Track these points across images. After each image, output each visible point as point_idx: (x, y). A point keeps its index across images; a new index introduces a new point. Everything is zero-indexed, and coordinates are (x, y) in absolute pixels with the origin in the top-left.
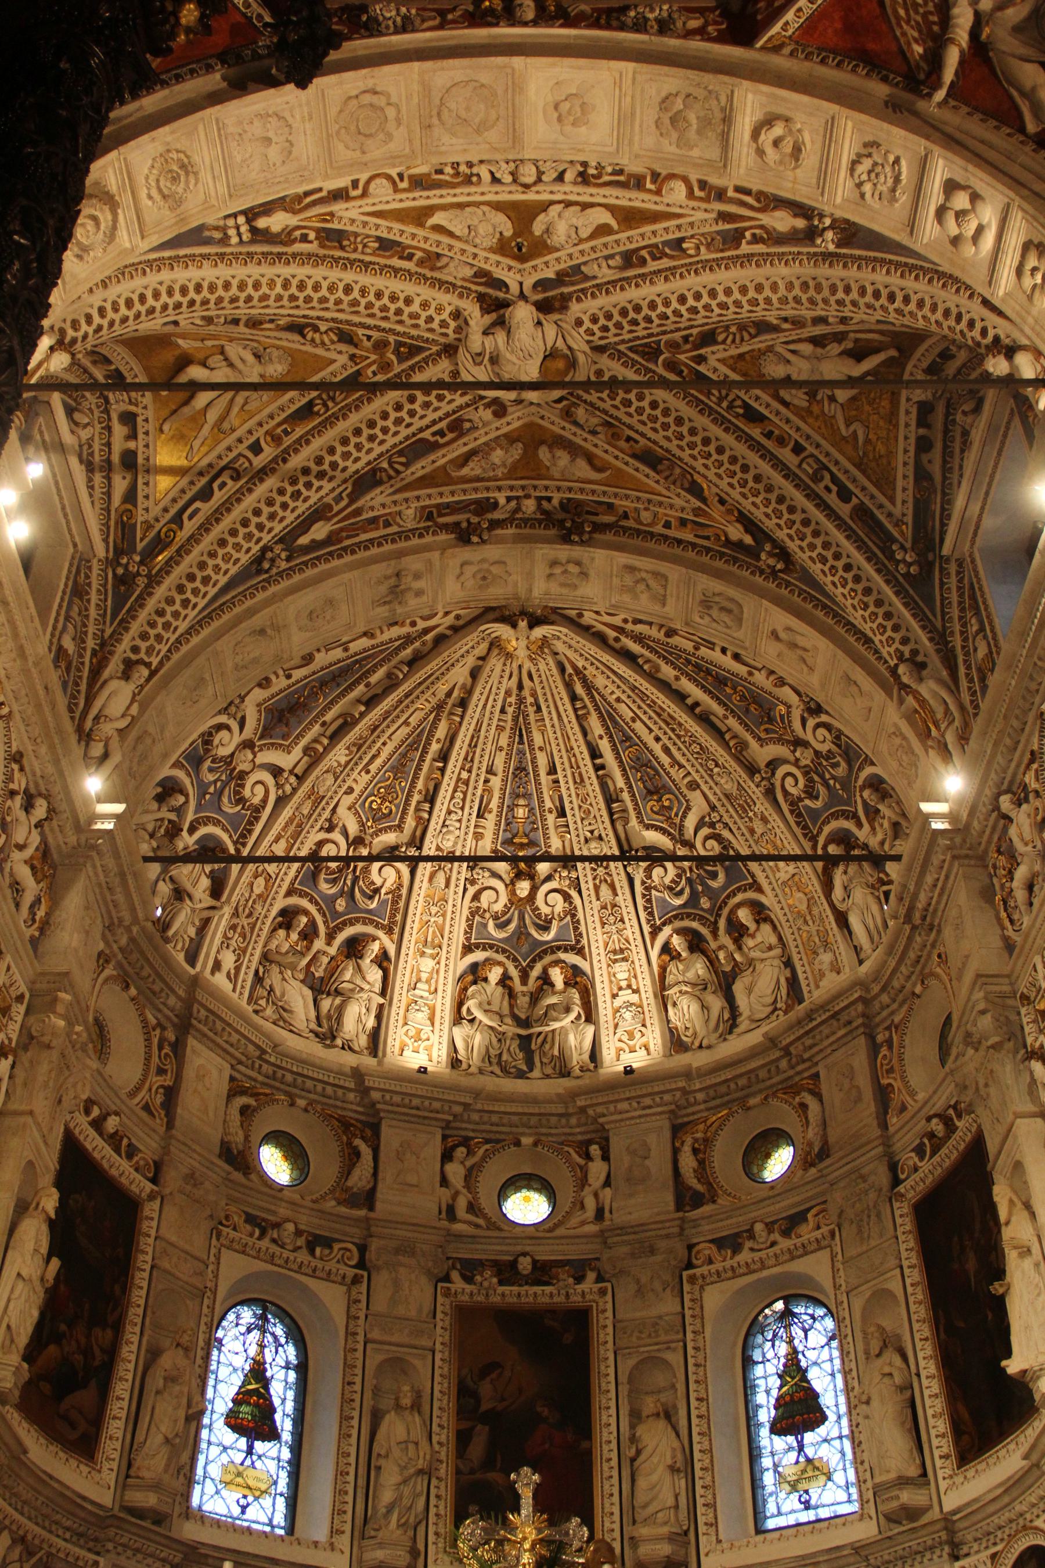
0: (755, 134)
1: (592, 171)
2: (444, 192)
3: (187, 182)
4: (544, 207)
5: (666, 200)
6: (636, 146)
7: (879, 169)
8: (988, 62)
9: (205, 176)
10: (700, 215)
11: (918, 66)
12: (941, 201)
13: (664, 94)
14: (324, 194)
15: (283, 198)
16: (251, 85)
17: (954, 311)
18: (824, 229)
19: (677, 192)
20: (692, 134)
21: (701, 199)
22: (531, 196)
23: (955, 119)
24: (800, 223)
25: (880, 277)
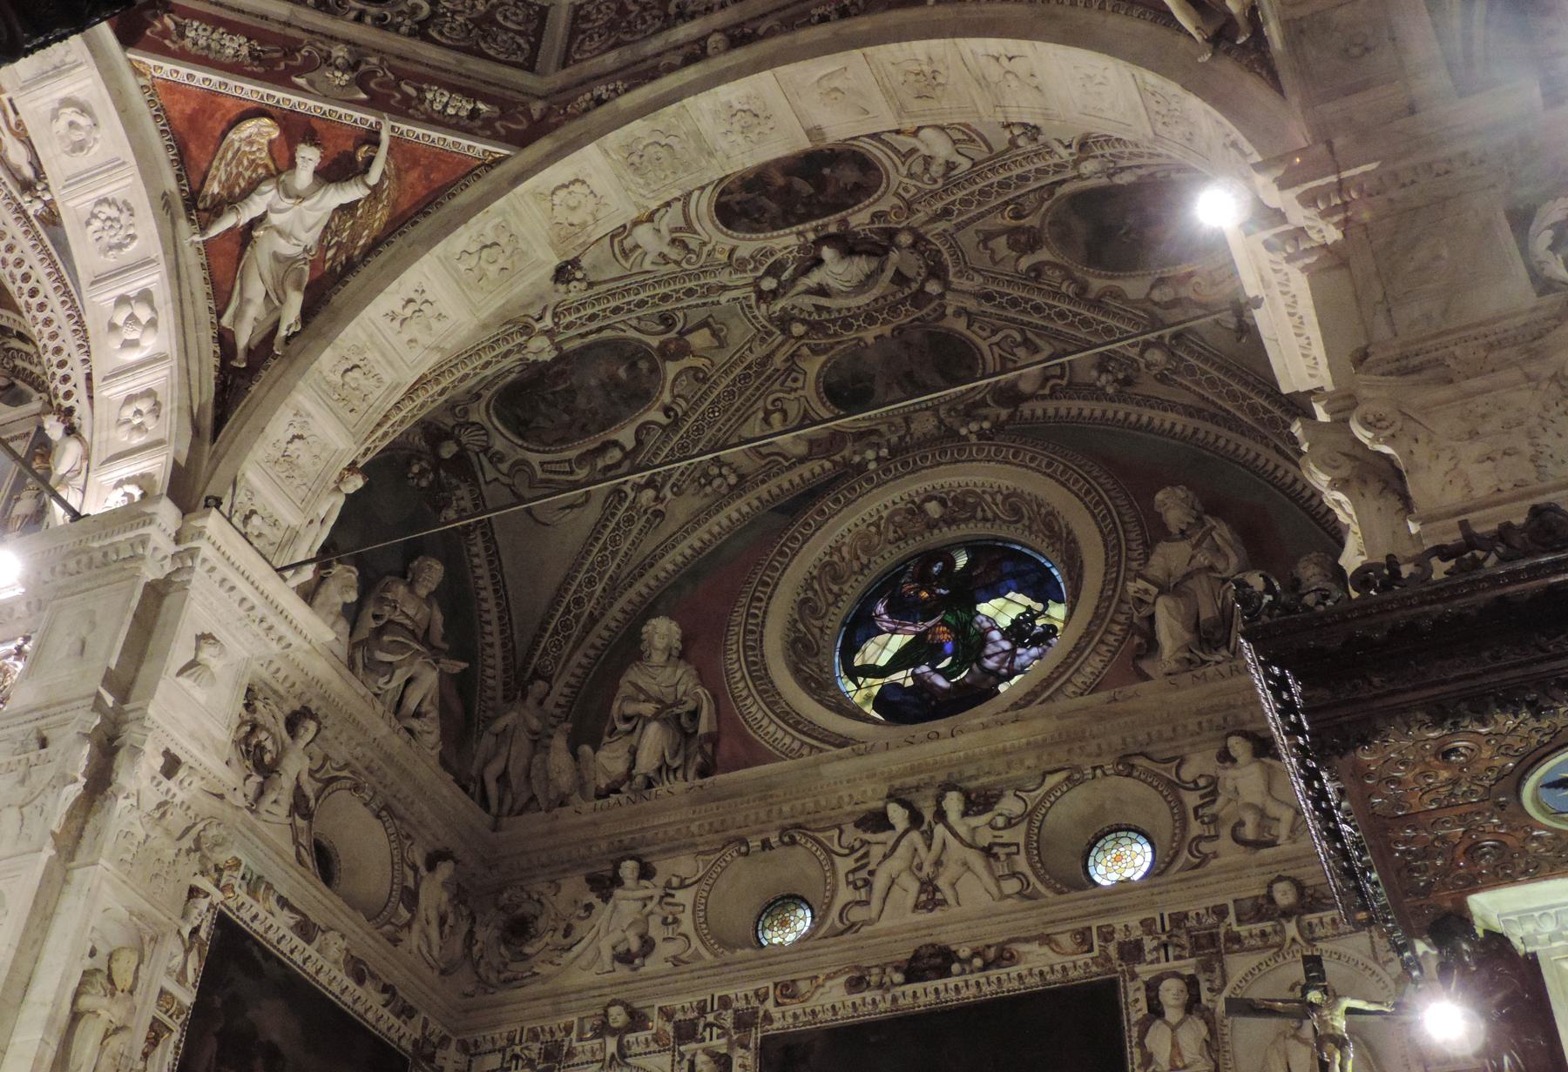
17: (64, 356)
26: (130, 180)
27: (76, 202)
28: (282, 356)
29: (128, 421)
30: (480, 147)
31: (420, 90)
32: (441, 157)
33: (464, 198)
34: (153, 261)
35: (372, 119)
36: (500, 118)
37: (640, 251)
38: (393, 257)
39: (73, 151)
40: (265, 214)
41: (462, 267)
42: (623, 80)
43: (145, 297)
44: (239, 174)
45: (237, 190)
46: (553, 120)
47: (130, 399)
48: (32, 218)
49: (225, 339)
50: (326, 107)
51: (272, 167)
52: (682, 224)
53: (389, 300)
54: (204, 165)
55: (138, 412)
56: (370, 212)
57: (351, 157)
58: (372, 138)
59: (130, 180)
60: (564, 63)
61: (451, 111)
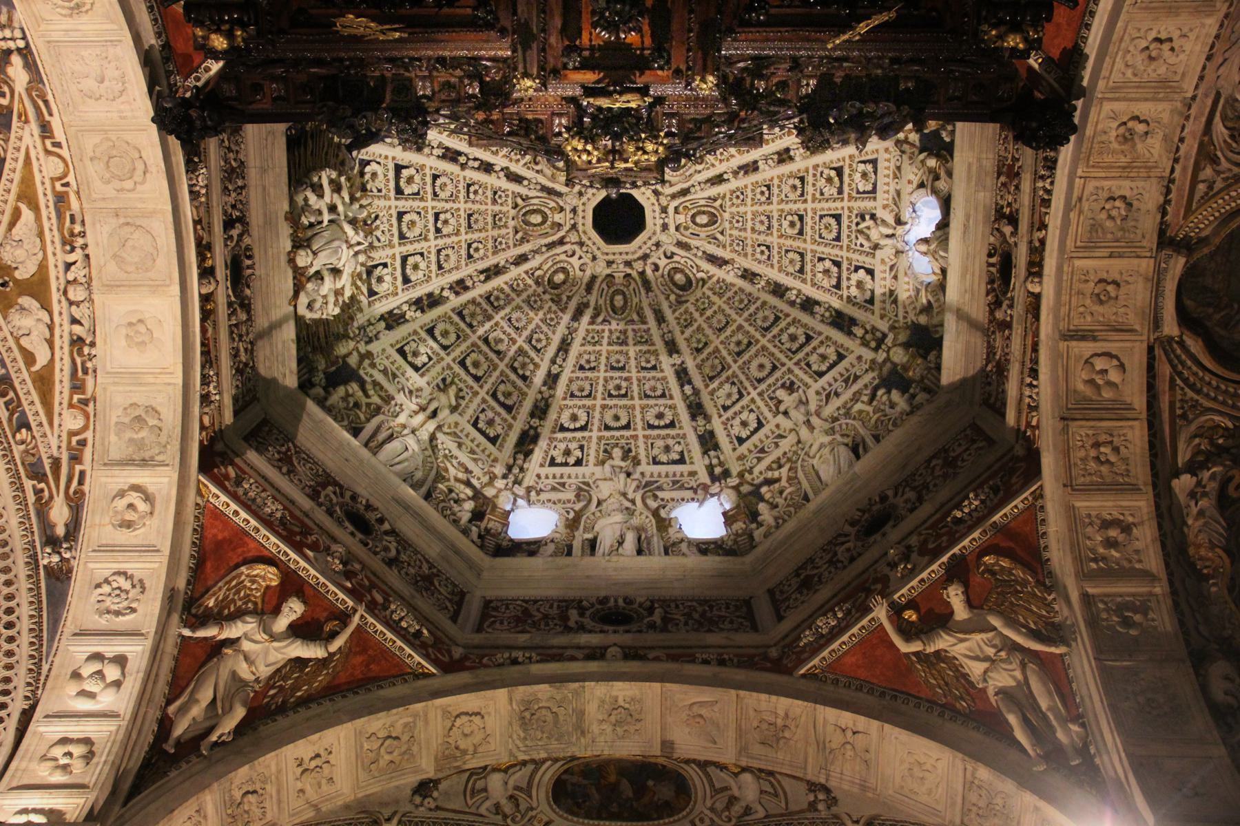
0: (136, 488)
1: (86, 350)
2: (54, 220)
3: (63, 7)
4: (46, 306)
5: (65, 412)
6: (112, 388)
7: (124, 596)
8: (209, 658)
9: (68, 23)
10: (54, 442)
11: (201, 605)
12: (108, 655)
13: (158, 408)
14: (47, 118)
15: (42, 81)
16: (147, 69)
18: (59, 553)
19: (72, 421)
20: (129, 434)
21: (69, 442)
22: (55, 296)
23: (170, 648)
24: (60, 531)
25: (25, 611)
26: (156, 565)
27: (98, 565)
28: (205, 757)
29: (56, 759)
30: (417, 658)
31: (386, 600)
32: (385, 653)
33: (388, 692)
34: (142, 635)
35: (350, 603)
36: (432, 646)
37: (484, 794)
38: (319, 715)
39: (121, 526)
40: (239, 639)
41: (366, 746)
42: (538, 654)
43: (121, 661)
44: (233, 601)
45: (226, 612)
46: (468, 664)
47: (64, 741)
48: (41, 568)
49: (165, 724)
50: (322, 580)
51: (260, 606)
52: (524, 785)
53: (302, 749)
54: (210, 583)
55: (69, 754)
56: (316, 673)
57: (320, 626)
58: (344, 618)
59: (156, 565)
60: (479, 629)
61: (404, 624)
